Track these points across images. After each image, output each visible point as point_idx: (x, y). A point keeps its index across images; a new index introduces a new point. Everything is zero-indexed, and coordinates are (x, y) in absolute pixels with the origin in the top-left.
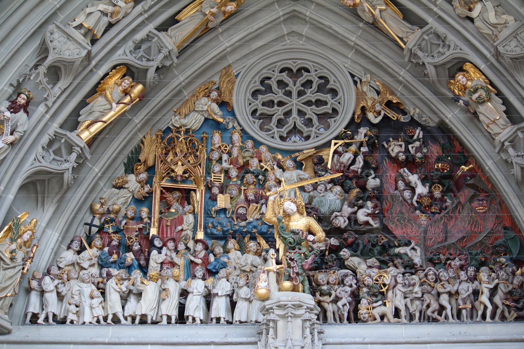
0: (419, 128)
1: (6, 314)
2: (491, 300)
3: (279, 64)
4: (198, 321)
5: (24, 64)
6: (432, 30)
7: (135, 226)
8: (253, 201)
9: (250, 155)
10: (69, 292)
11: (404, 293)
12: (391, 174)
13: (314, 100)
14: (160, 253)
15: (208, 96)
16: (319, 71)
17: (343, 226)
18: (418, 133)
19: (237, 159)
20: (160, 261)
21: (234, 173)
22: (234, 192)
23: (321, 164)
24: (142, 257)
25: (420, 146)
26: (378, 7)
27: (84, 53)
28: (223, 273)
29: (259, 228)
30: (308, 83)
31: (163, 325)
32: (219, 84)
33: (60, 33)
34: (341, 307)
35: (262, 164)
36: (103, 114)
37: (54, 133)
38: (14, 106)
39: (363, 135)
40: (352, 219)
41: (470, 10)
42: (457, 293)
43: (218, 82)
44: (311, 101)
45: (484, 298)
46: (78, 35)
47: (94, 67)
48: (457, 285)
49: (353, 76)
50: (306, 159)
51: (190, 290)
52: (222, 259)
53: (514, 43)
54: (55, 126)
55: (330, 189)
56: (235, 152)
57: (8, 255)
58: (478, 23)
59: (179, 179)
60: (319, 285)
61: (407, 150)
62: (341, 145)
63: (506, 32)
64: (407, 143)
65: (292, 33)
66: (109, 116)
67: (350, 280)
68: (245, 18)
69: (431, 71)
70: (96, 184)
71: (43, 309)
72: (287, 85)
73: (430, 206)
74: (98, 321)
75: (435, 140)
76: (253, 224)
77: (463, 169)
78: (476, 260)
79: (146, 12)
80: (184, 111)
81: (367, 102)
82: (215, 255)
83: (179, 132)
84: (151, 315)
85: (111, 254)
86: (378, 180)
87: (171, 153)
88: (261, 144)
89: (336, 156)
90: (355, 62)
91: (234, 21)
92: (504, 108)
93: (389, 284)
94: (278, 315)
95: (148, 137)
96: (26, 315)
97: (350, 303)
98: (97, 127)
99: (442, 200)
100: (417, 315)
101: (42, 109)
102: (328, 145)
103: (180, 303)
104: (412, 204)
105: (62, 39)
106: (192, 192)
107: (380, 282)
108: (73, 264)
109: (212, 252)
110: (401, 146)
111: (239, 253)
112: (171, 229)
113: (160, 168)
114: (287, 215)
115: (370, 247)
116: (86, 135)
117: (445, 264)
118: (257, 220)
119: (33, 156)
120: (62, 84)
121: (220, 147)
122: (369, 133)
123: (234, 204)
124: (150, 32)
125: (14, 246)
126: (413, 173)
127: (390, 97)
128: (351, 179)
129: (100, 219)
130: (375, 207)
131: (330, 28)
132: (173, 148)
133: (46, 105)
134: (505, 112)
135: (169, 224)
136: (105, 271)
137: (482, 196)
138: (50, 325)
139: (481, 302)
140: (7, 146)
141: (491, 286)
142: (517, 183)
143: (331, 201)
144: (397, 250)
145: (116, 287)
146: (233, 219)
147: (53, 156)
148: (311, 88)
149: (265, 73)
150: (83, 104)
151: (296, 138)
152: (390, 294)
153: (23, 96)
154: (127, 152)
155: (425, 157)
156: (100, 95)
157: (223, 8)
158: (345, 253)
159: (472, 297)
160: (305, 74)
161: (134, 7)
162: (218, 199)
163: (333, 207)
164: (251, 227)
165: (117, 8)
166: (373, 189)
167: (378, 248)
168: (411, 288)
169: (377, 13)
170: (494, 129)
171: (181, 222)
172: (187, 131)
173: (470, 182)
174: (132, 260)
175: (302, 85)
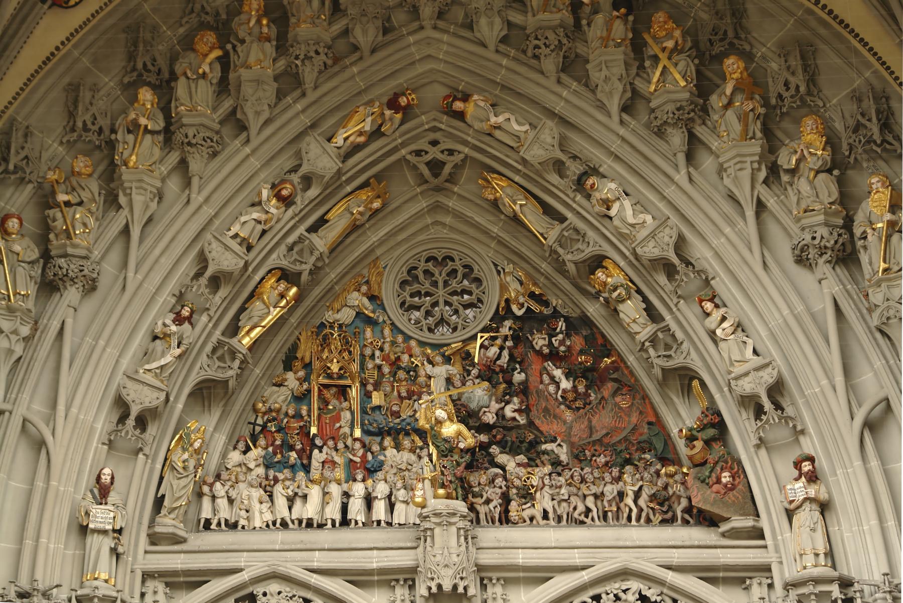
0: (562, 319)
1: (181, 522)
3: (424, 253)
5: (184, 274)
8: (405, 398)
9: (401, 349)
10: (239, 495)
12: (535, 365)
13: (459, 291)
14: (321, 452)
16: (464, 260)
17: (491, 423)
18: (561, 325)
20: (322, 460)
21: (386, 370)
23: (468, 358)
24: (305, 457)
25: (564, 339)
27: (242, 263)
29: (413, 425)
30: (453, 272)
35: (412, 359)
36: (262, 318)
37: (216, 340)
38: (178, 318)
39: (508, 328)
40: (500, 414)
44: (457, 291)
49: (496, 265)
50: (453, 354)
54: (218, 333)
56: (387, 347)
59: (335, 376)
61: (550, 342)
62: (486, 339)
64: (551, 336)
65: (436, 223)
66: (268, 321)
68: (392, 212)
72: (433, 275)
73: (575, 400)
76: (407, 421)
77: (606, 361)
81: (510, 293)
82: (372, 453)
83: (332, 327)
86: (523, 375)
88: (411, 338)
89: (482, 350)
91: (380, 215)
98: (257, 332)
101: (204, 318)
102: (474, 338)
103: (343, 503)
104: (557, 399)
105: (219, 249)
109: (370, 450)
111: (395, 451)
112: (330, 427)
116: (246, 341)
117: (591, 460)
118: (410, 416)
119: (198, 365)
120: (223, 292)
121: (372, 342)
122: (513, 326)
123: (388, 401)
124: (301, 234)
125: (186, 456)
126: (557, 368)
127: (533, 289)
133: (208, 315)
136: (271, 473)
138: (222, 531)
140: (175, 359)
142: (658, 381)
143: (479, 397)
145: (283, 492)
146: (387, 416)
147: (218, 363)
148: (456, 278)
150: (242, 309)
151: (444, 329)
153: (187, 309)
155: (569, 348)
156: (258, 298)
157: (369, 206)
160: (450, 263)
162: (373, 396)
163: (481, 404)
164: (404, 423)
166: (519, 384)
171: (338, 419)
173: (612, 376)
175: (448, 275)
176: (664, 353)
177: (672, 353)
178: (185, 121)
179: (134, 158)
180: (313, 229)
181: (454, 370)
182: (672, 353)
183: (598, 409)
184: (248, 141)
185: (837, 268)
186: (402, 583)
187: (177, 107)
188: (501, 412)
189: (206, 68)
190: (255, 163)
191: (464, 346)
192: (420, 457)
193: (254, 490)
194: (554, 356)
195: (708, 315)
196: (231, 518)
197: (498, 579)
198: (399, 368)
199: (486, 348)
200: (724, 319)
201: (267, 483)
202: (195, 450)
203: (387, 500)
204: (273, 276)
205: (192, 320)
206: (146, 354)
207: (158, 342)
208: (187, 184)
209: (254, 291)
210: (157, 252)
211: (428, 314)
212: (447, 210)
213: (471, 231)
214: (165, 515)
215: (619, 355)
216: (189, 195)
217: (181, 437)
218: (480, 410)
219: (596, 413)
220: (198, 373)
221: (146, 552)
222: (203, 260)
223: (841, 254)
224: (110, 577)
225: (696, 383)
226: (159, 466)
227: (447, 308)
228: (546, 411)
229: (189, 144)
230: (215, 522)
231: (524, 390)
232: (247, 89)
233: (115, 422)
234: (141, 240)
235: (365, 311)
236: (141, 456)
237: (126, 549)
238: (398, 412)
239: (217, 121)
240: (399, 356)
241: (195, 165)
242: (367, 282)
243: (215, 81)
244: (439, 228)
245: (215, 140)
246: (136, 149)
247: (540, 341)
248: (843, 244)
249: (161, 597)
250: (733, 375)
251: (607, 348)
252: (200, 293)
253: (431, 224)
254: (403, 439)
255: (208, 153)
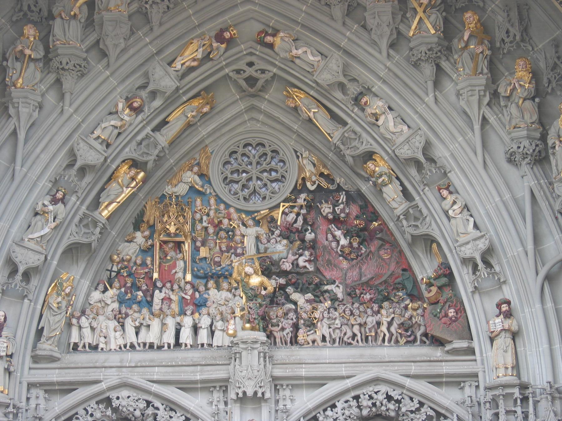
0: (344, 193)
1: (56, 346)
2: (388, 329)
3: (242, 141)
4: (189, 346)
6: (351, 129)
7: (142, 271)
11: (329, 325)
13: (268, 170)
14: (161, 292)
15: (192, 170)
16: (272, 147)
17: (288, 270)
18: (343, 197)
19: (213, 220)
21: (211, 230)
22: (212, 245)
25: (344, 208)
26: (313, 110)
28: (204, 310)
30: (265, 154)
31: (165, 350)
32: (199, 159)
33: (85, 144)
34: (286, 335)
36: (118, 196)
39: (303, 199)
40: (295, 264)
41: (377, 120)
42: (365, 323)
43: (198, 158)
45: (384, 328)
46: (96, 144)
47: (110, 162)
48: (365, 318)
49: (296, 152)
50: (262, 218)
51: (182, 324)
52: (204, 295)
53: (406, 147)
54: (84, 208)
55: (280, 241)
56: (212, 213)
57: (55, 305)
58: (382, 130)
59: (172, 235)
60: (271, 319)
61: (334, 210)
62: (287, 207)
63: (401, 139)
64: (334, 206)
65: (252, 119)
66: (122, 198)
67: (292, 315)
68: (218, 113)
69: (350, 160)
70: (115, 241)
71: (81, 340)
73: (350, 253)
74: (120, 348)
75: (354, 201)
78: (381, 295)
79: (144, 120)
80: (175, 182)
81: (306, 173)
82: (199, 292)
84: (156, 342)
85: (126, 293)
87: (166, 216)
89: (283, 216)
90: (298, 142)
92: (401, 188)
93: (319, 318)
94: (242, 348)
95: (149, 203)
96: (69, 344)
97: (291, 332)
99: (359, 249)
100: (338, 340)
101: (74, 198)
102: (278, 206)
103: (176, 329)
104: (337, 252)
105: (85, 148)
106: (182, 245)
107: (313, 316)
108: (100, 301)
109: (197, 290)
110: (330, 208)
113: (159, 226)
114: (248, 275)
115: (307, 285)
116: (105, 213)
118: (228, 265)
119: (69, 232)
120: (88, 179)
122: (307, 198)
125: (59, 299)
126: (339, 229)
128: (294, 233)
129: (117, 266)
130: (311, 255)
131: (279, 118)
132: (168, 212)
133: (77, 196)
134: (401, 191)
135: (166, 268)
137: (387, 246)
139: (381, 331)
141: (389, 319)
144: (326, 288)
147: (84, 230)
149: (233, 148)
150: (103, 189)
152: (319, 324)
154: (135, 215)
155: (348, 215)
156: (114, 181)
158: (290, 290)
159: (376, 326)
161: (137, 116)
163: (281, 255)
164: (224, 270)
165: (124, 122)
166: (310, 241)
167: (312, 286)
168: (333, 321)
169: (311, 115)
170: (394, 205)
171: (174, 266)
172: (177, 197)
173: (378, 236)
174: (141, 297)
175: (260, 157)
176: (414, 223)
177: (418, 223)
178: (60, 51)
179: (20, 81)
180: (157, 129)
181: (262, 230)
182: (418, 223)
183: (367, 260)
184: (108, 65)
185: (535, 168)
186: (218, 389)
187: (54, 41)
188: (295, 263)
189: (76, 10)
190: (113, 81)
191: (270, 213)
192: (235, 296)
193: (110, 322)
194: (336, 220)
195: (445, 199)
196: (93, 342)
197: (287, 385)
198: (221, 229)
199: (287, 214)
200: (454, 203)
201: (120, 316)
202: (66, 294)
203: (209, 328)
204: (126, 164)
205: (65, 200)
206: (29, 226)
207: (38, 217)
208: (62, 97)
209: (111, 175)
210: (38, 150)
211: (244, 186)
212: (260, 111)
213: (278, 126)
214: (44, 342)
215: (384, 221)
216: (63, 107)
217: (56, 284)
218: (281, 260)
219: (365, 263)
220: (69, 238)
221: (30, 369)
222: (72, 156)
223: (537, 158)
224: (4, 388)
225: (434, 246)
226: (39, 307)
227: (259, 182)
228: (329, 263)
229: (63, 69)
230: (81, 345)
231: (313, 245)
232: (108, 28)
233: (7, 275)
234: (26, 141)
235: (196, 186)
236: (26, 301)
237: (16, 368)
238: (220, 262)
239: (84, 50)
240: (221, 221)
241: (68, 83)
242: (198, 164)
243: (83, 20)
244: (254, 122)
245: (83, 66)
246: (23, 74)
247: (326, 209)
248: (539, 152)
249: (42, 401)
250: (458, 244)
251: (376, 216)
252: (70, 180)
253: (248, 120)
254: (223, 281)
255: (77, 75)
